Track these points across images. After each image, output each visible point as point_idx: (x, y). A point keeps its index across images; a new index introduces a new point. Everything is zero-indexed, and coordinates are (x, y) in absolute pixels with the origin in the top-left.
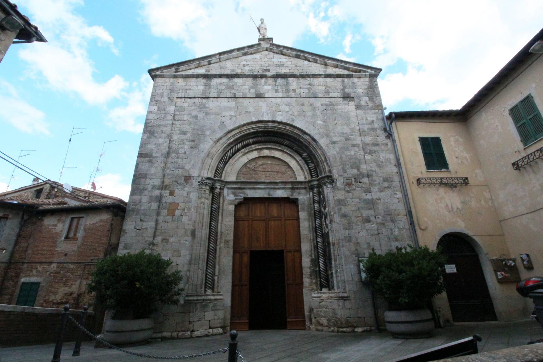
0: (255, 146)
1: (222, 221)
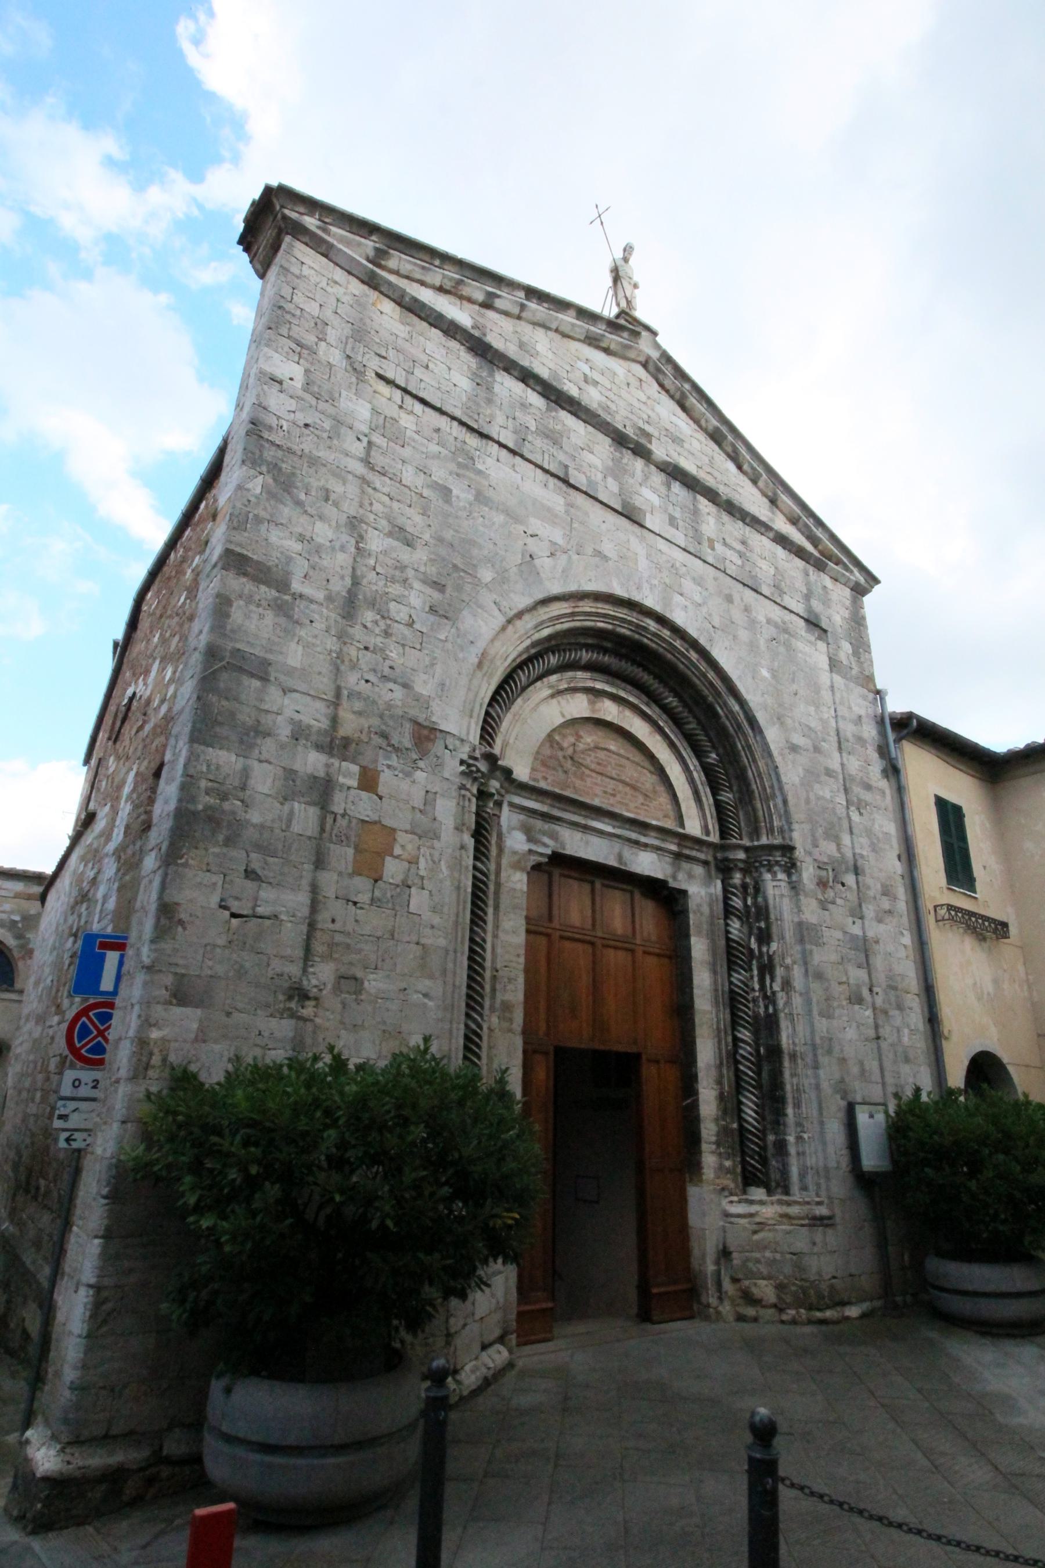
0: (588, 675)
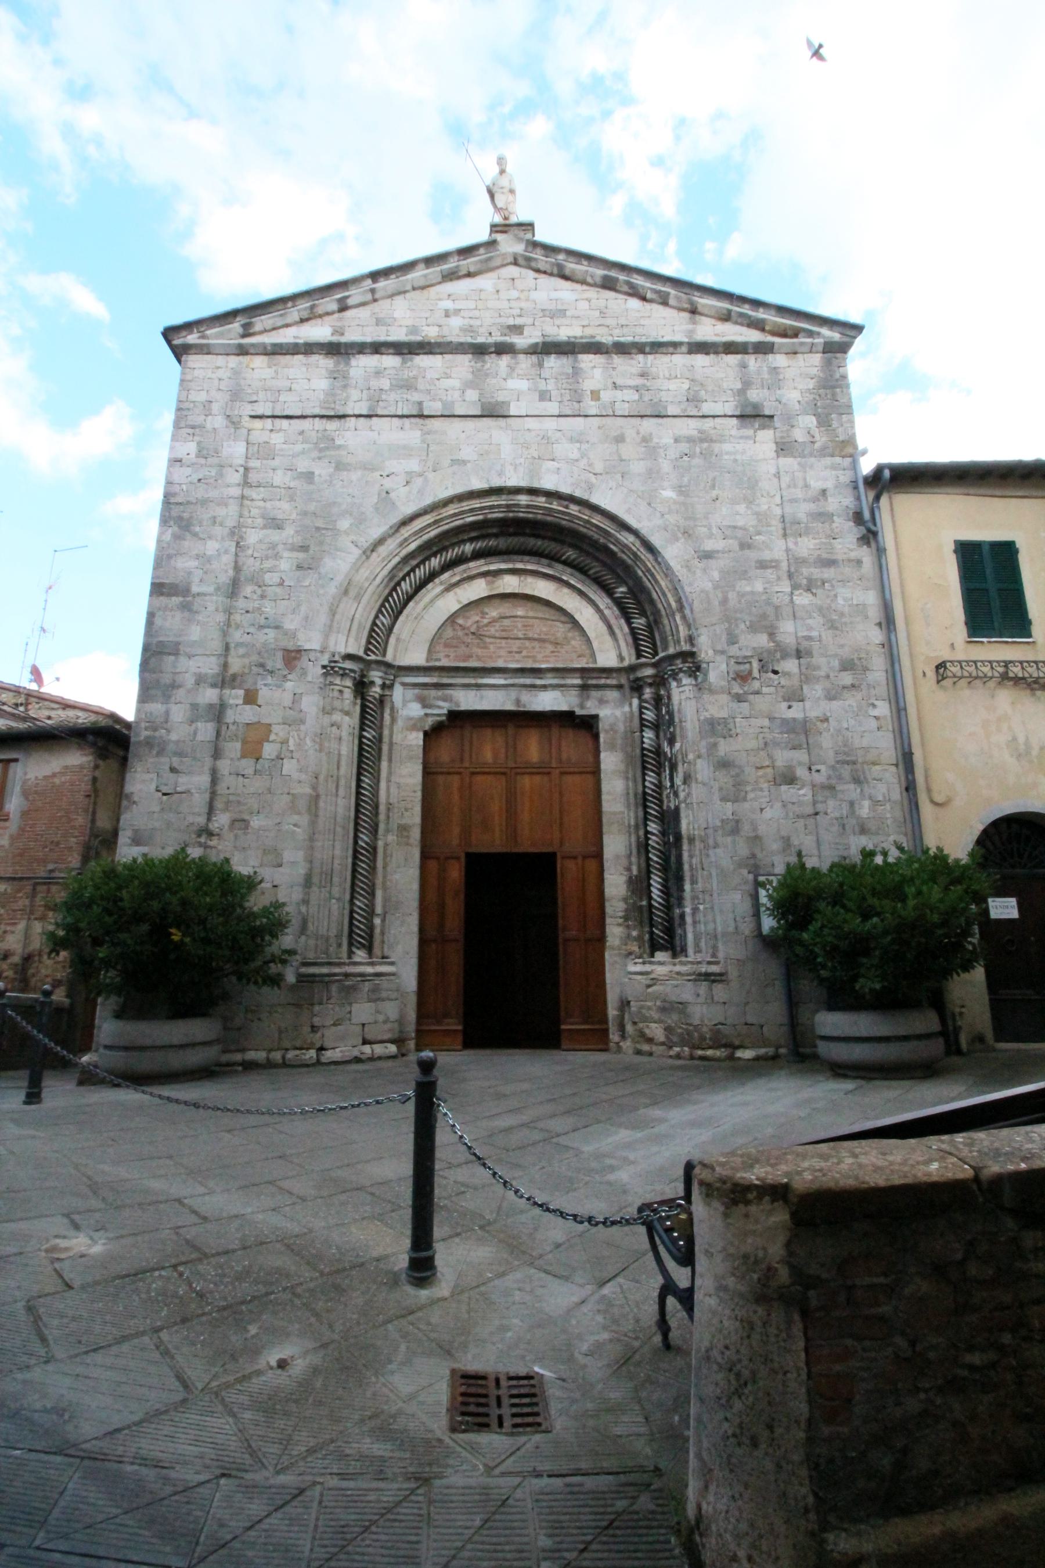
0: (482, 561)
1: (390, 773)
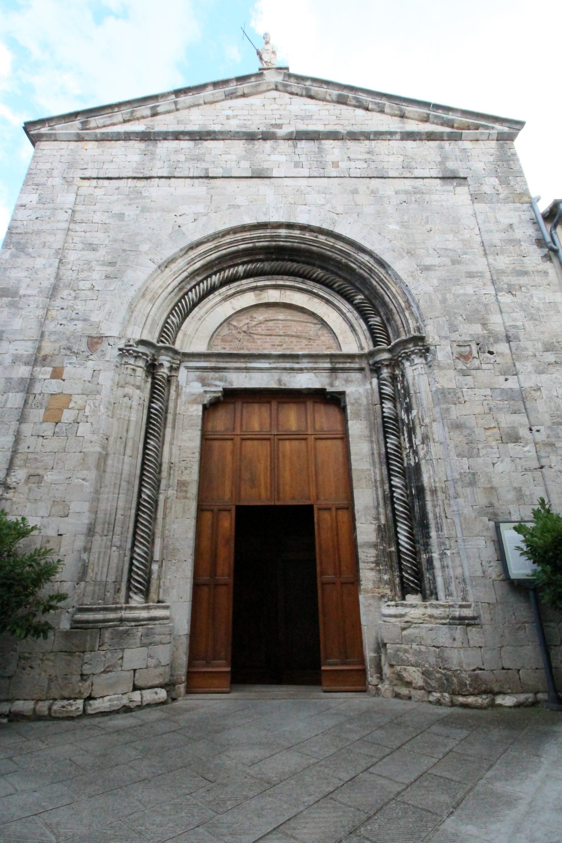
1: (173, 438)
